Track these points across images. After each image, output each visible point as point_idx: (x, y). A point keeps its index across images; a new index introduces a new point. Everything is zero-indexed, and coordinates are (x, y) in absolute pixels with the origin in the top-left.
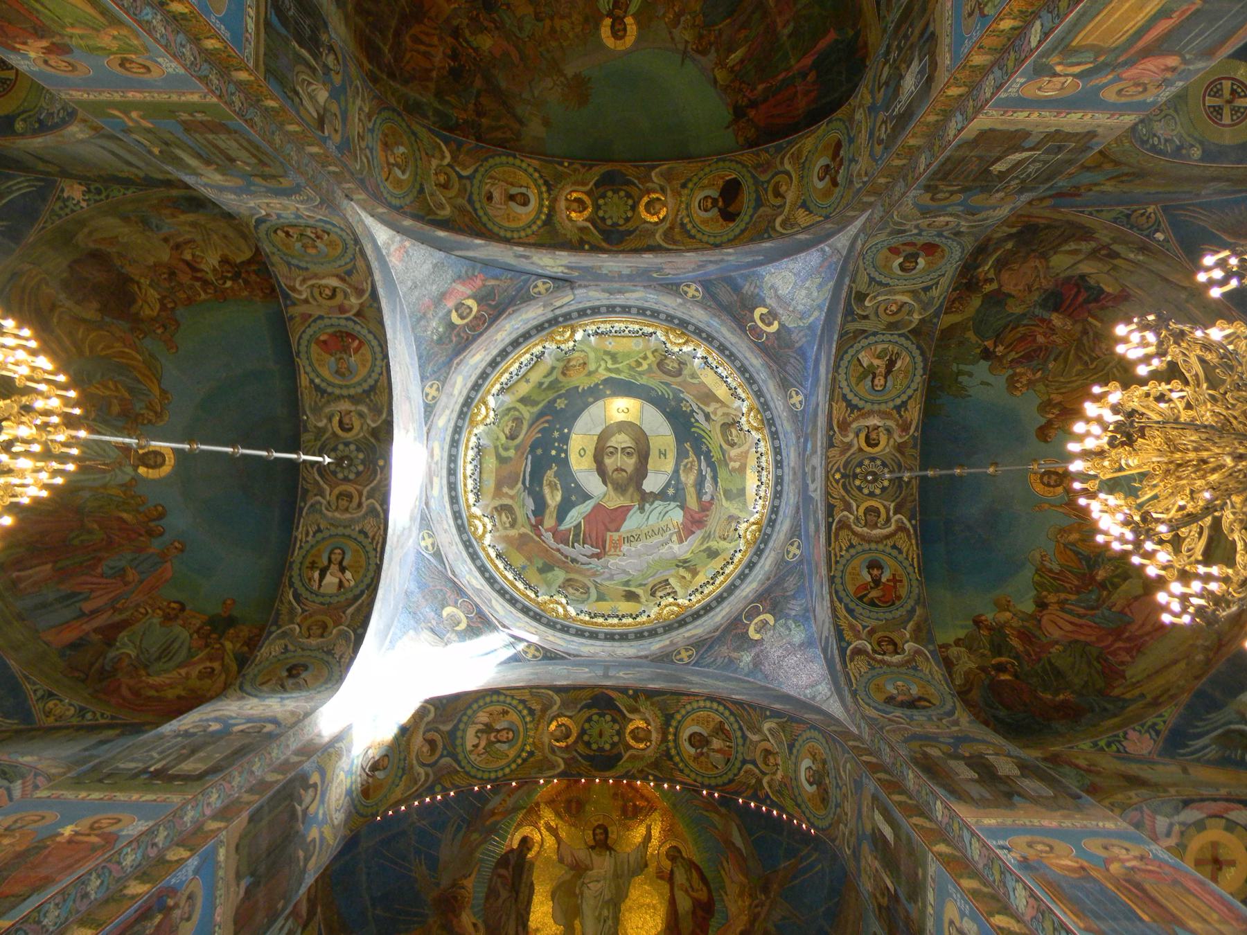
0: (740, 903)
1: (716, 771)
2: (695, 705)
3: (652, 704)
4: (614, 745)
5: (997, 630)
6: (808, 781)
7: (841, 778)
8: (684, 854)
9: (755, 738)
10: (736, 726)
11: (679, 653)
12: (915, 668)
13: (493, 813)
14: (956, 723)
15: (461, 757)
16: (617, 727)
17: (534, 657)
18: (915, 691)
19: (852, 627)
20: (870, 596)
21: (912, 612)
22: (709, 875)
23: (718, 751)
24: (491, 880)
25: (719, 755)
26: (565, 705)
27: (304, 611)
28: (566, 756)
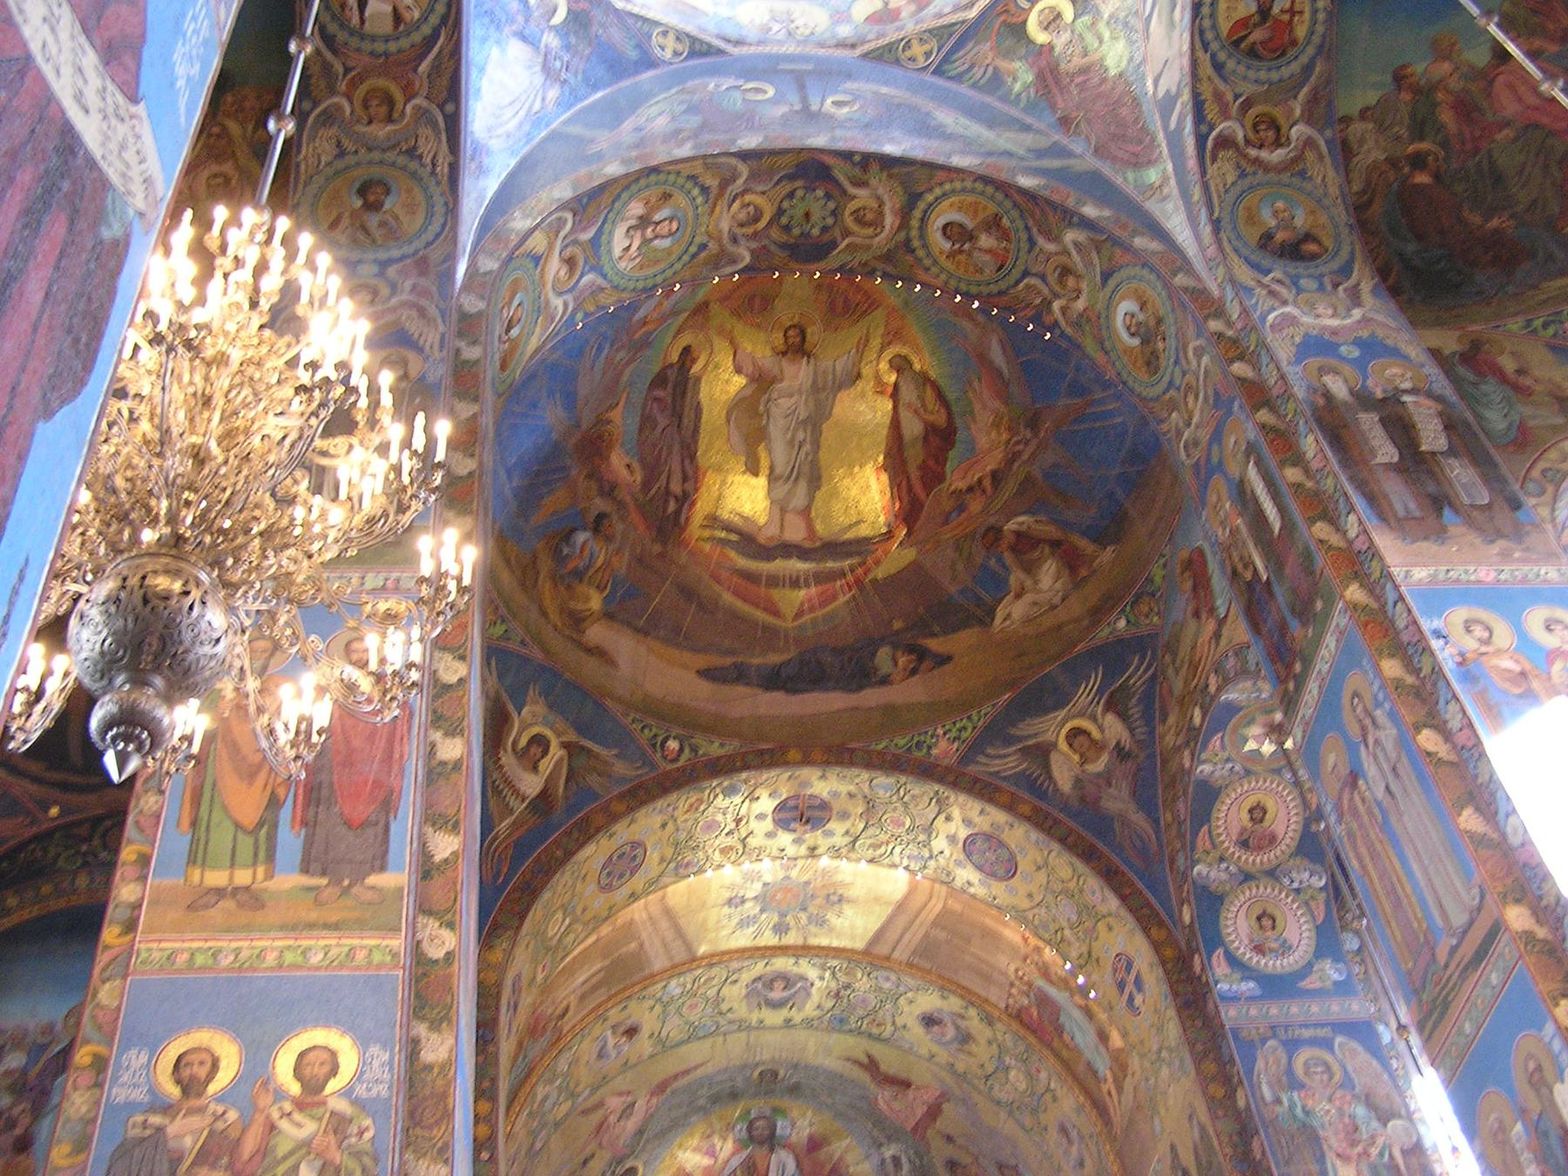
0: (994, 434)
1: (978, 277)
2: (958, 185)
3: (890, 176)
4: (825, 229)
5: (1424, 93)
6: (1128, 328)
7: (1188, 363)
8: (917, 367)
9: (1051, 247)
10: (1020, 224)
11: (908, 45)
12: (1302, 174)
13: (645, 323)
14: (1355, 298)
15: (607, 269)
16: (831, 205)
17: (676, 54)
18: (1299, 221)
19: (1218, 96)
20: (1251, 39)
21: (1308, 69)
22: (951, 396)
23: (989, 251)
24: (644, 409)
25: (987, 257)
26: (753, 176)
27: (347, 70)
28: (754, 245)
